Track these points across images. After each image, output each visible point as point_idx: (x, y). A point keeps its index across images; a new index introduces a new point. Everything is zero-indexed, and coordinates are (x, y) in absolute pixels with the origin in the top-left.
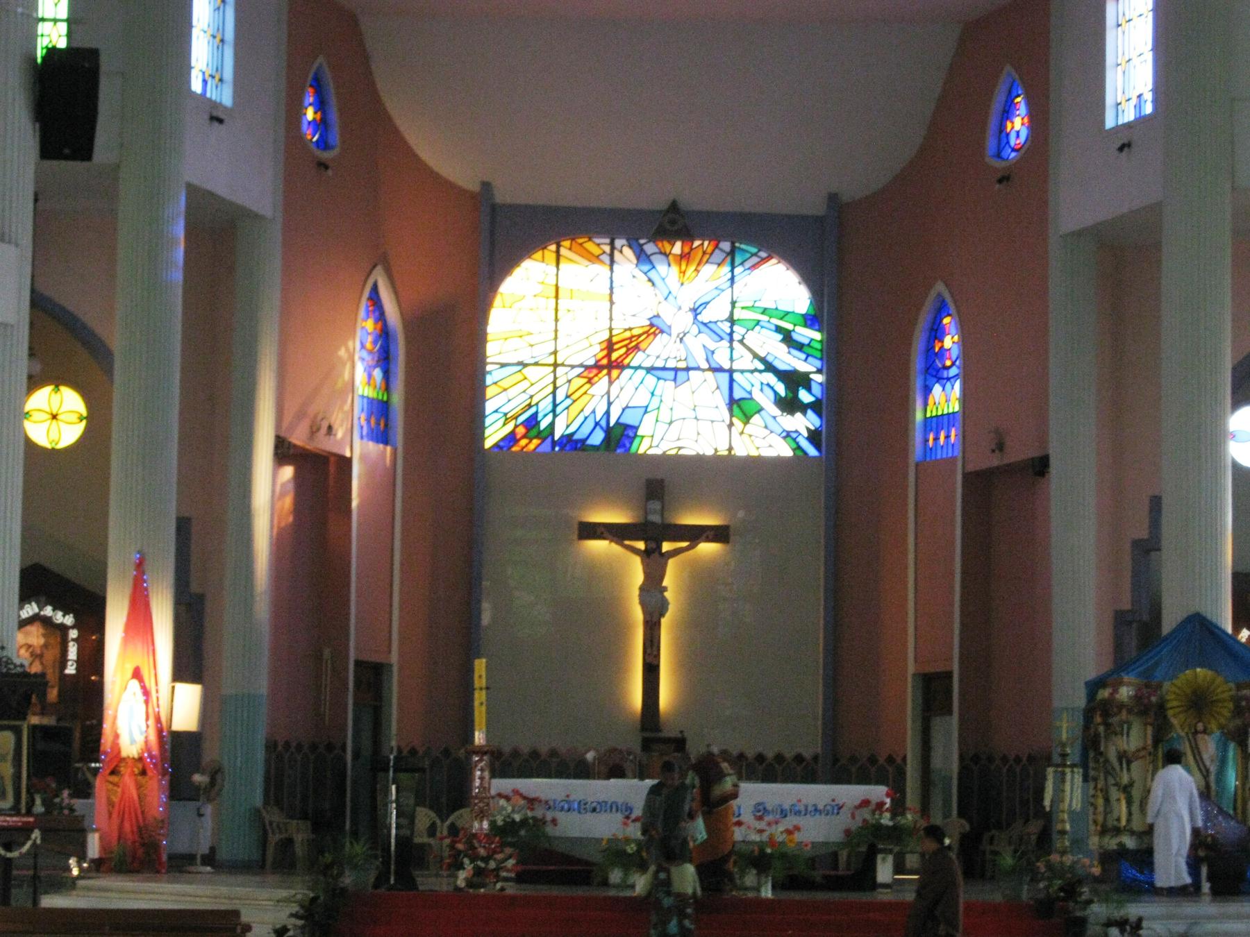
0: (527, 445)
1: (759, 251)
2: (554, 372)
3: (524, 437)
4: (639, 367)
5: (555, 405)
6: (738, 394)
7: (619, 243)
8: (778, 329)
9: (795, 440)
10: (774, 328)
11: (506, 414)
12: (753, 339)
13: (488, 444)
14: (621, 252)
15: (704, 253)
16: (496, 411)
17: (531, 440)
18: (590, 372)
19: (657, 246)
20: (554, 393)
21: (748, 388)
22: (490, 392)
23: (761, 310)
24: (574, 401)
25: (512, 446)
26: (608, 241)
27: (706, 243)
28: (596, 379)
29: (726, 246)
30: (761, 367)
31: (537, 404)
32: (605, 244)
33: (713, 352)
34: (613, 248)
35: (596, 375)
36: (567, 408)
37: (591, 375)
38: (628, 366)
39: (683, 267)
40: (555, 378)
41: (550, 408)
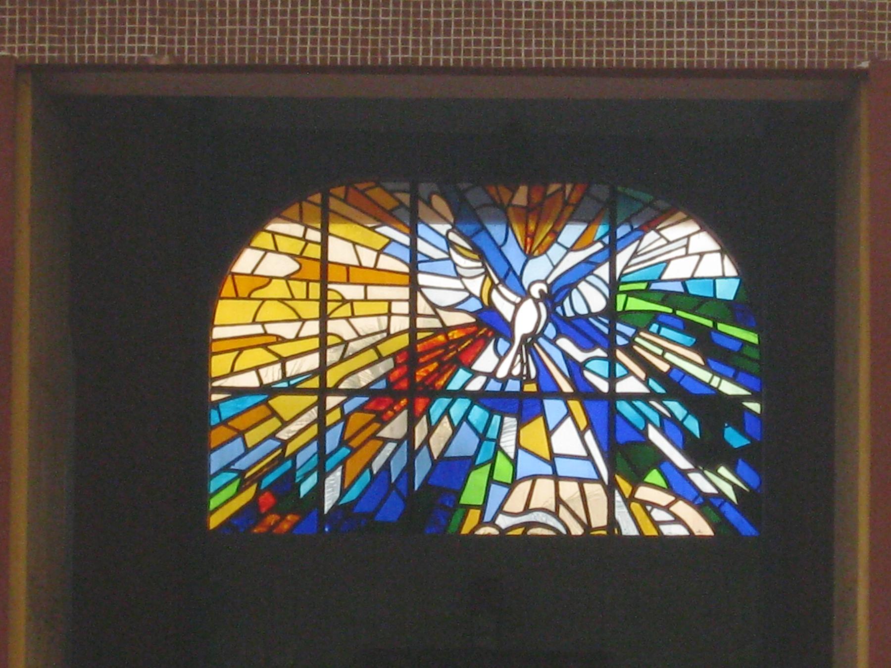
0: (277, 523)
1: (656, 199)
2: (321, 404)
3: (271, 511)
4: (462, 393)
5: (322, 456)
6: (624, 434)
7: (424, 189)
8: (688, 328)
9: (717, 510)
10: (681, 326)
11: (241, 473)
12: (646, 344)
13: (215, 521)
14: (429, 204)
15: (566, 204)
16: (226, 468)
17: (283, 518)
18: (378, 404)
19: (487, 192)
20: (320, 438)
21: (640, 423)
22: (217, 436)
23: (659, 297)
24: (354, 451)
25: (254, 526)
26: (406, 185)
27: (569, 188)
28: (390, 413)
29: (602, 191)
30: (659, 389)
31: (294, 456)
32: (404, 191)
33: (582, 366)
34: (415, 198)
35: (391, 407)
36: (343, 462)
37: (382, 408)
38: (444, 392)
39: (532, 227)
40: (323, 412)
41: (315, 461)
